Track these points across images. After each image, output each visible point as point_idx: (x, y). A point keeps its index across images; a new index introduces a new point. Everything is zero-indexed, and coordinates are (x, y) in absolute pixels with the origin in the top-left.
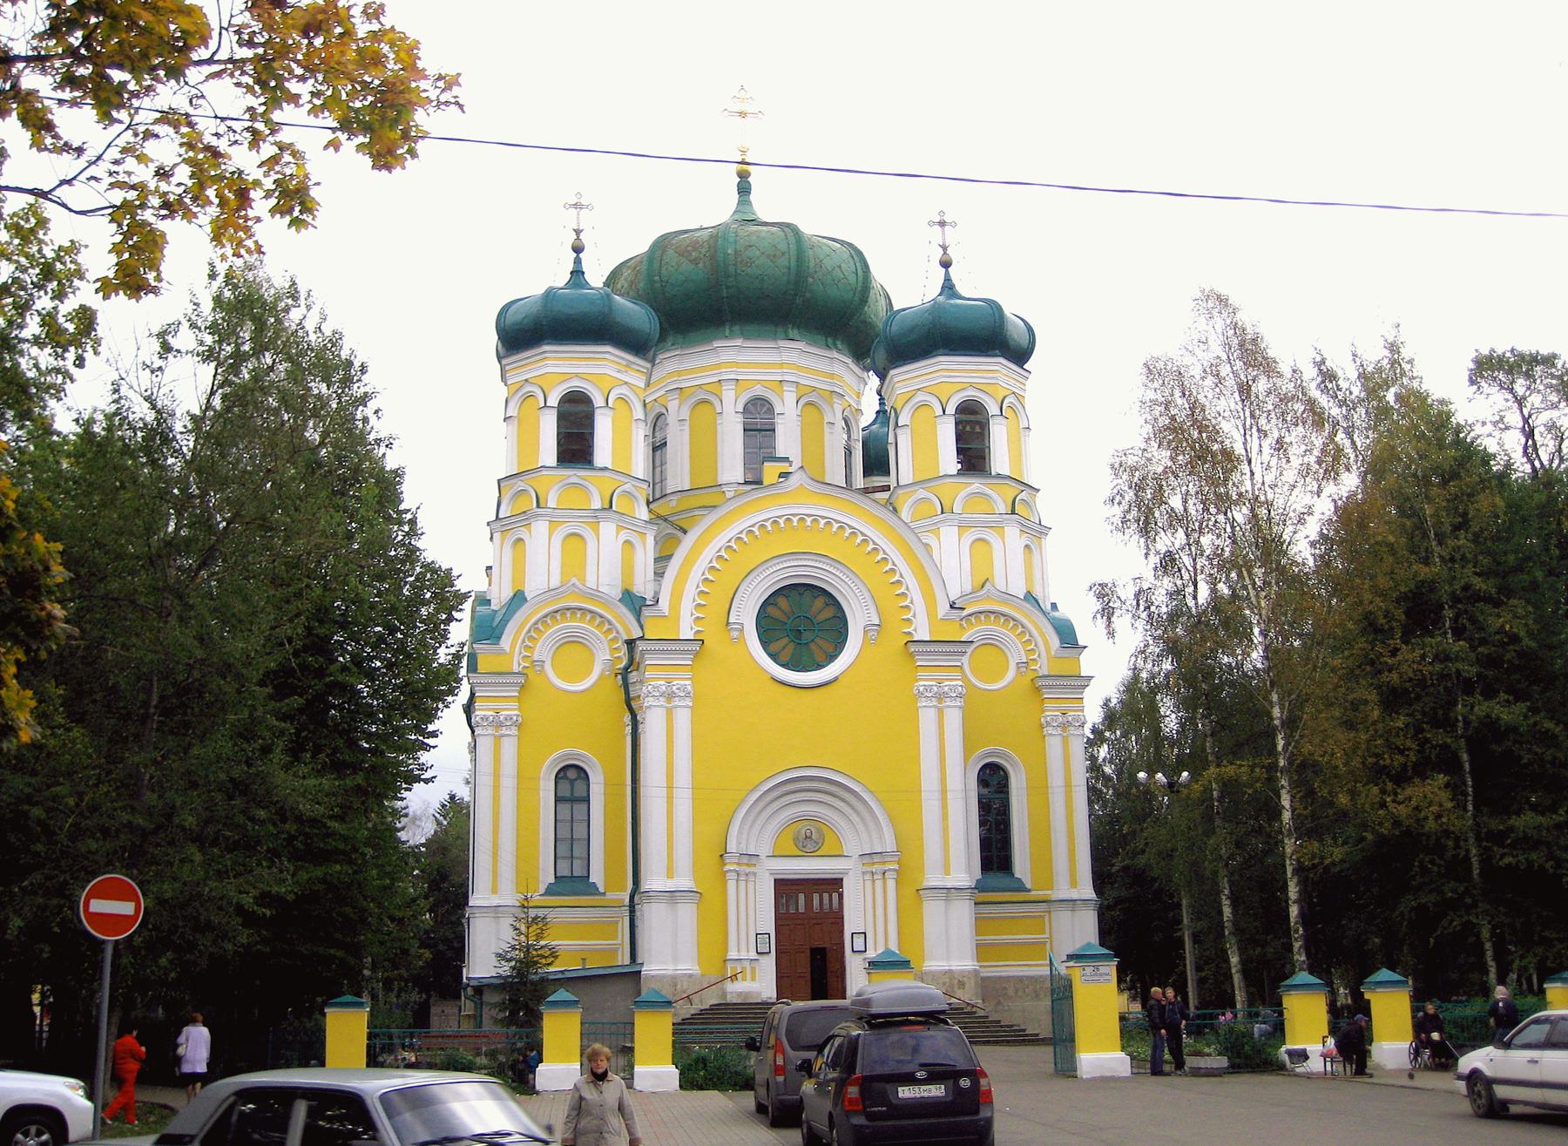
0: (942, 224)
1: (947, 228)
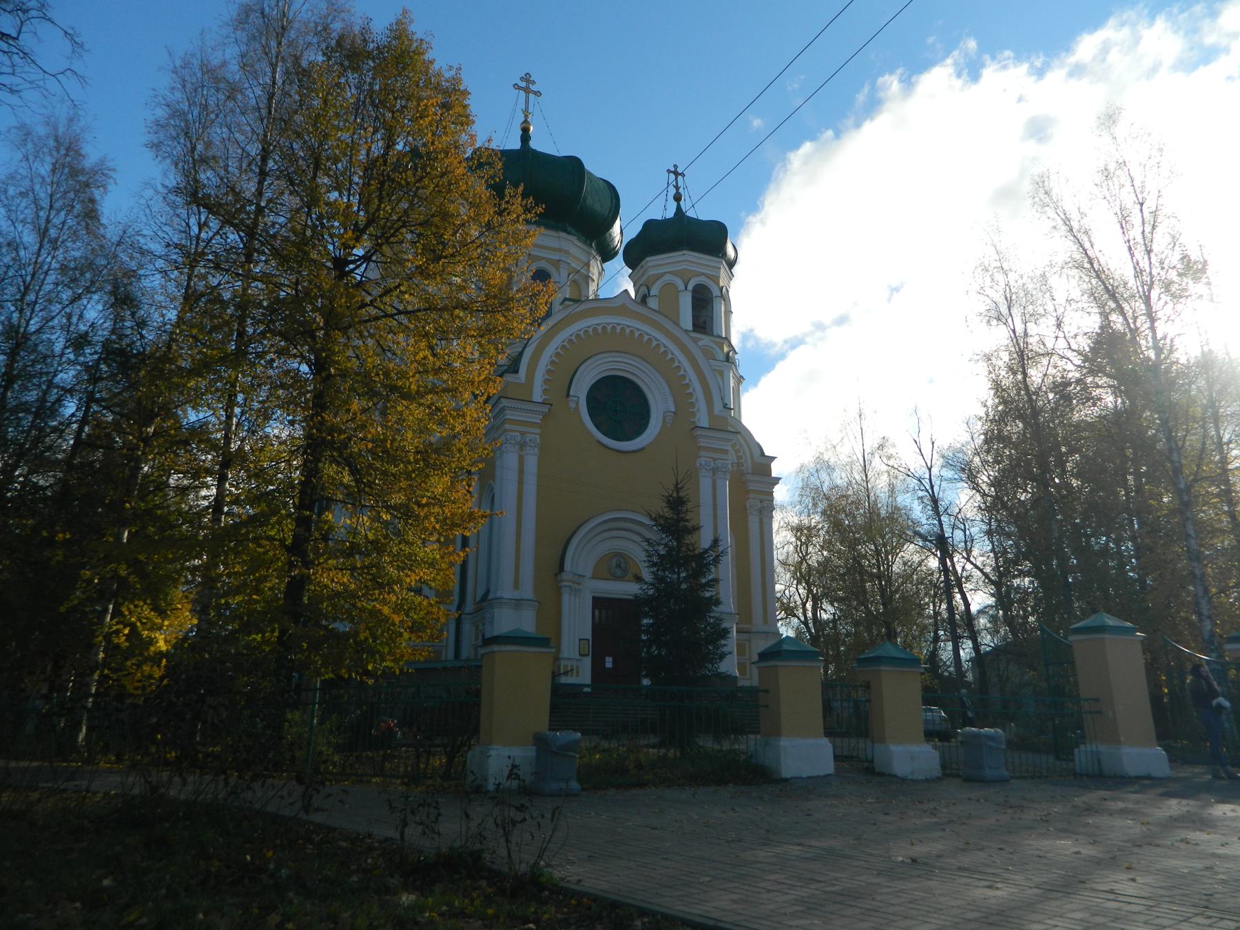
0: (676, 173)
1: (680, 178)
